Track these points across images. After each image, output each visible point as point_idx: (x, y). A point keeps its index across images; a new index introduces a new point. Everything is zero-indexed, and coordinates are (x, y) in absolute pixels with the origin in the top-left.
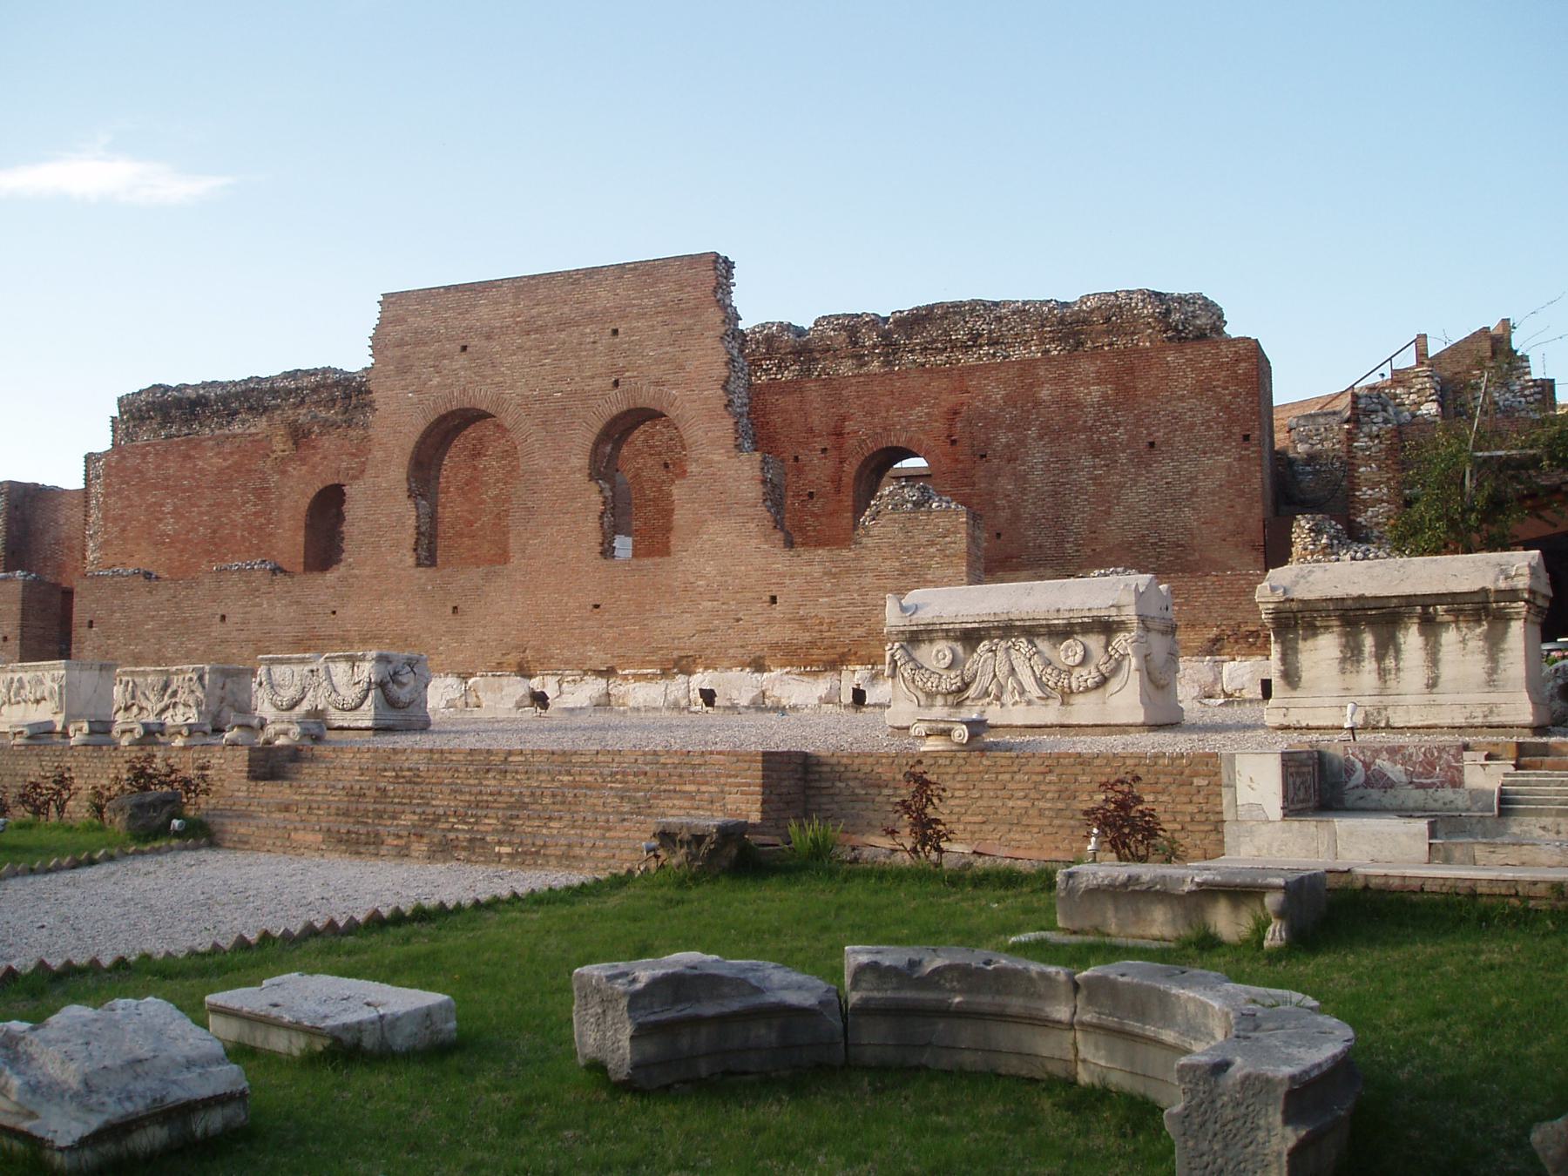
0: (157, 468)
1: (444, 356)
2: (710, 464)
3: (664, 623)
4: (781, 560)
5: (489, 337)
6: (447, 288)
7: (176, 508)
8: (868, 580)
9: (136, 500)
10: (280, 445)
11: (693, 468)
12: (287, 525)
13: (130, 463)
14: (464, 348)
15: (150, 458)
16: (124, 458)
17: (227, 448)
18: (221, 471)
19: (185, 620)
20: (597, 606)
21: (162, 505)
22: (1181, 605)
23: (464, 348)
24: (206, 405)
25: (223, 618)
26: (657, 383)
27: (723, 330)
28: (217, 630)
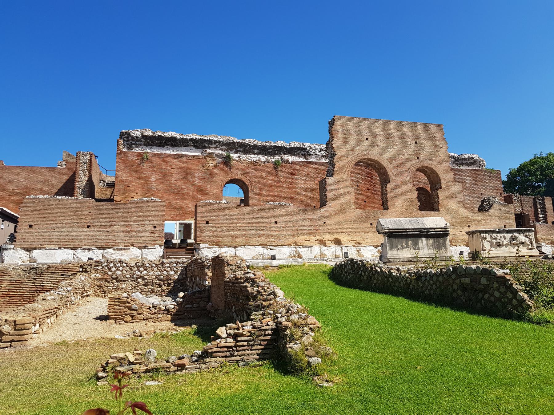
4: (470, 215)
5: (375, 137)
7: (157, 180)
9: (135, 175)
11: (443, 186)
12: (214, 191)
18: (181, 168)
19: (258, 223)
21: (150, 178)
24: (174, 141)
25: (276, 223)
26: (430, 160)
28: (274, 227)
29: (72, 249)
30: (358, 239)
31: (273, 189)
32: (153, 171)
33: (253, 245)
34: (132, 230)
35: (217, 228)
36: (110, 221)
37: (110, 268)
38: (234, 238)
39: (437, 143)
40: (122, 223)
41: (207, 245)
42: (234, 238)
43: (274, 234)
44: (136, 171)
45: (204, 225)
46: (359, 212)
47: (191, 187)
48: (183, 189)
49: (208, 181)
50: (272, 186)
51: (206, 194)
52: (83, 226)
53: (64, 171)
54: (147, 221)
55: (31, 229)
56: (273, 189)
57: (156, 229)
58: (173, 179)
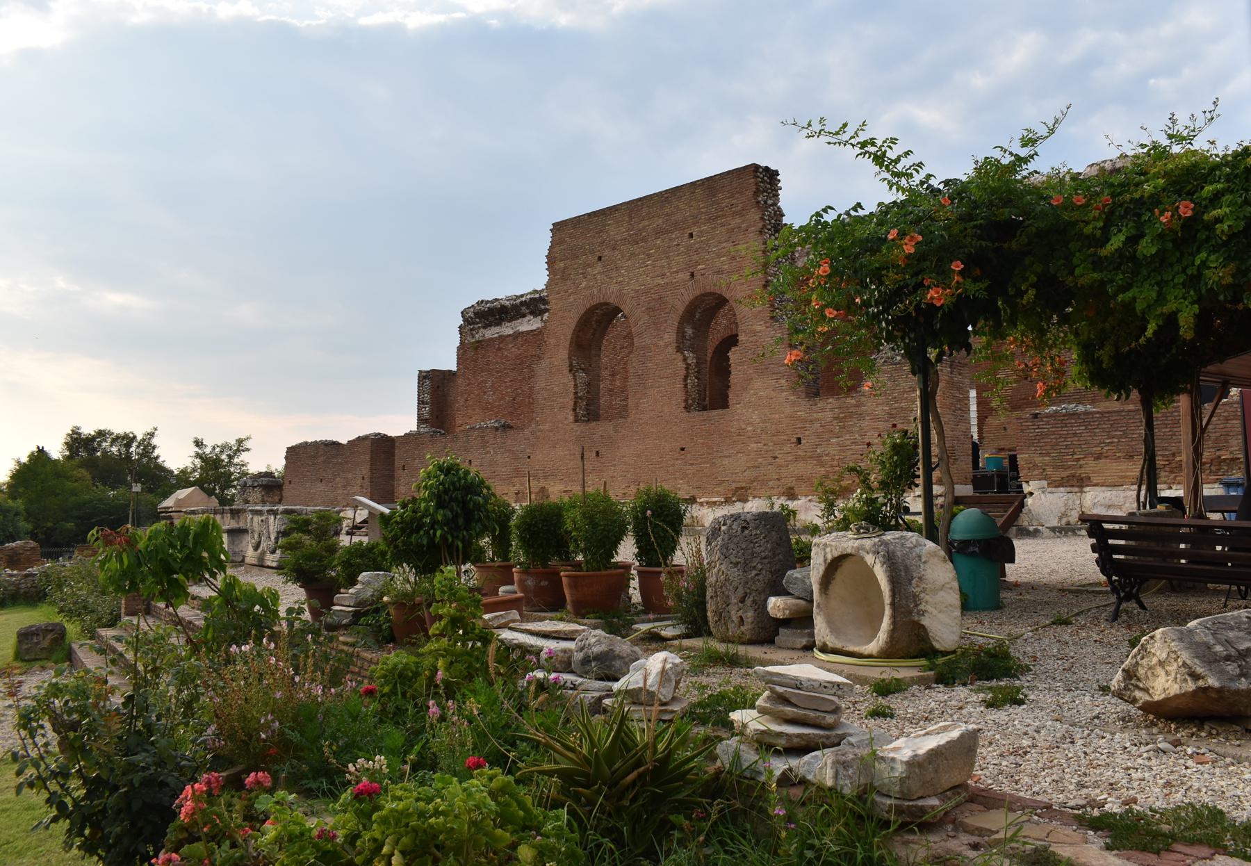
1: (588, 265)
2: (754, 333)
3: (726, 461)
4: (803, 409)
6: (589, 215)
8: (865, 423)
14: (600, 259)
20: (683, 449)
22: (1119, 437)
23: (600, 259)
27: (760, 225)
39: (736, 221)
48: (518, 394)
58: (508, 380)
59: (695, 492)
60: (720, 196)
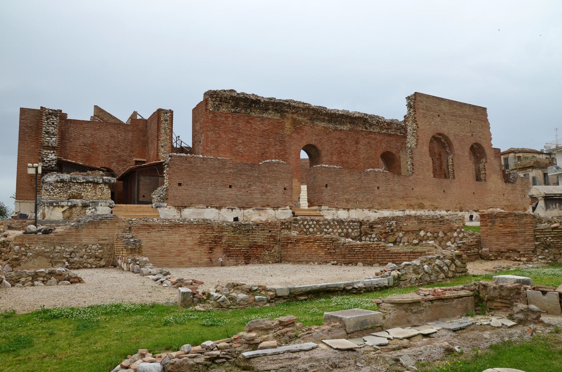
0: (233, 124)
3: (487, 199)
6: (433, 97)
7: (243, 142)
9: (223, 136)
10: (288, 125)
12: (293, 156)
13: (219, 119)
15: (230, 119)
16: (216, 116)
17: (266, 122)
18: (264, 131)
19: (365, 187)
21: (237, 139)
23: (439, 116)
24: (258, 104)
25: (378, 187)
28: (377, 192)
29: (217, 208)
30: (436, 204)
31: (342, 156)
32: (239, 133)
33: (362, 208)
34: (267, 191)
35: (335, 192)
36: (248, 181)
37: (305, 226)
38: (348, 201)
40: (258, 184)
41: (327, 207)
42: (348, 201)
43: (377, 198)
44: (224, 132)
45: (324, 188)
46: (436, 180)
47: (273, 150)
48: (266, 152)
49: (287, 145)
50: (341, 153)
51: (287, 158)
52: (225, 186)
53: (129, 128)
54: (279, 182)
55: (181, 188)
56: (342, 156)
57: (286, 191)
59: (479, 208)
60: (478, 113)
